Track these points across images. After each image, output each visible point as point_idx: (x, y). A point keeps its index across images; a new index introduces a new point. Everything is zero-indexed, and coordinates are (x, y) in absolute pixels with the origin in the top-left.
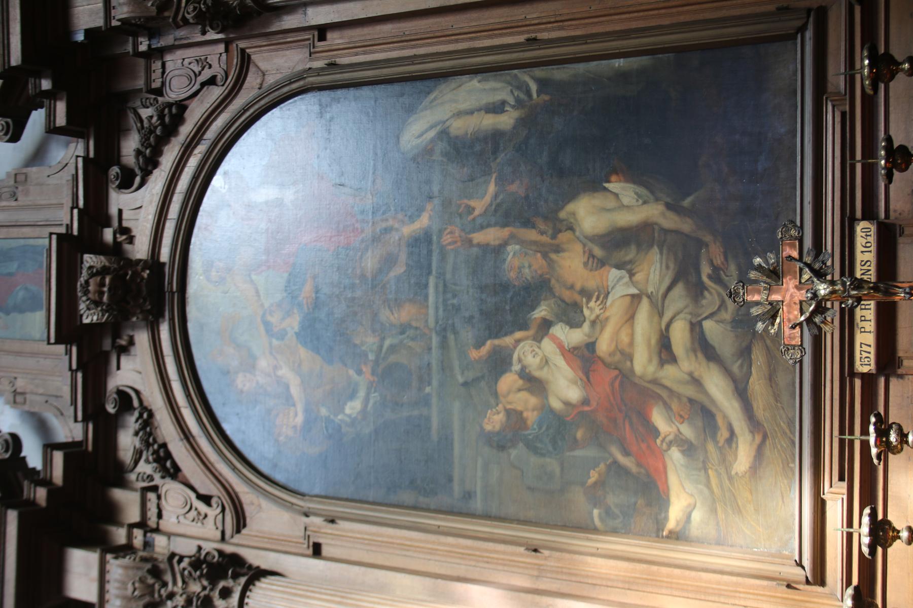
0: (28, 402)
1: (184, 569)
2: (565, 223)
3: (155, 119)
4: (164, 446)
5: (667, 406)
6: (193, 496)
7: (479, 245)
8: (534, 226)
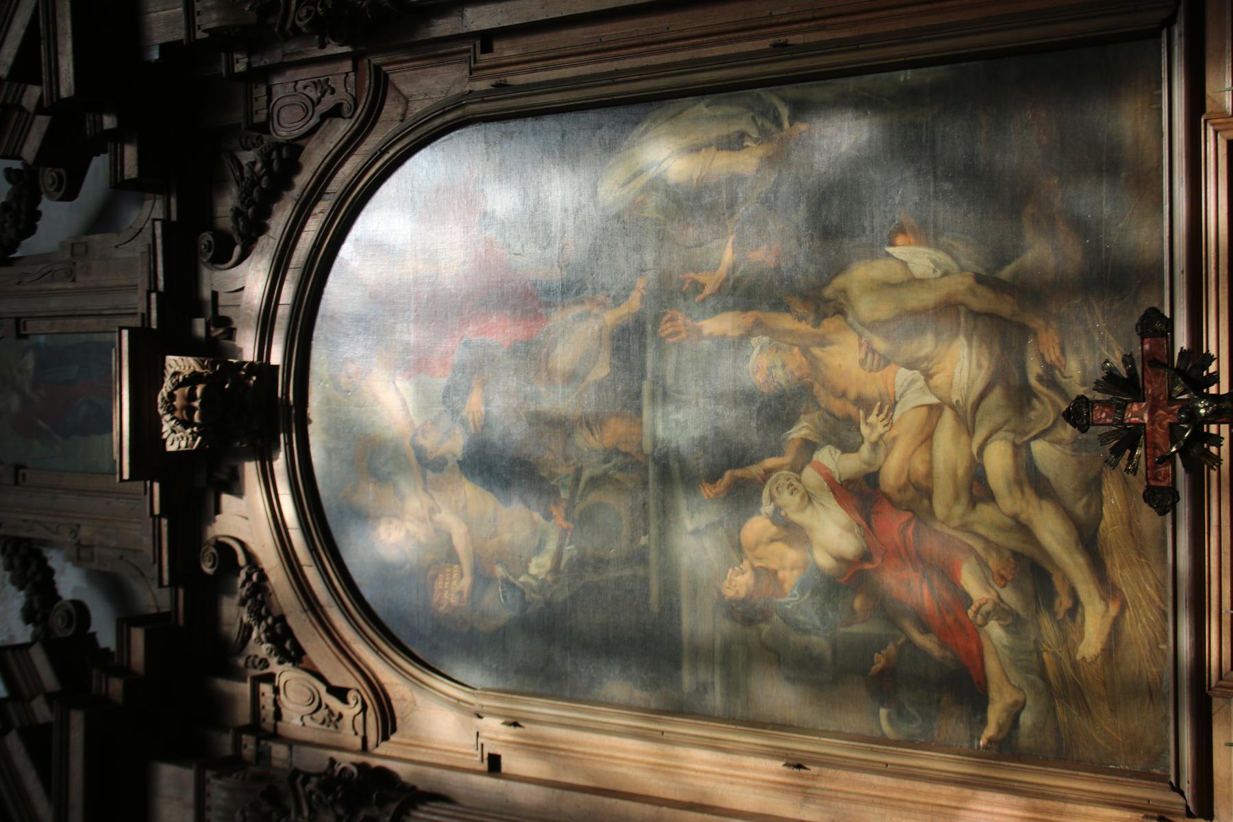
1: (311, 793)
2: (832, 304)
3: (259, 166)
4: (281, 619)
5: (982, 563)
6: (322, 688)
7: (711, 336)
8: (788, 310)
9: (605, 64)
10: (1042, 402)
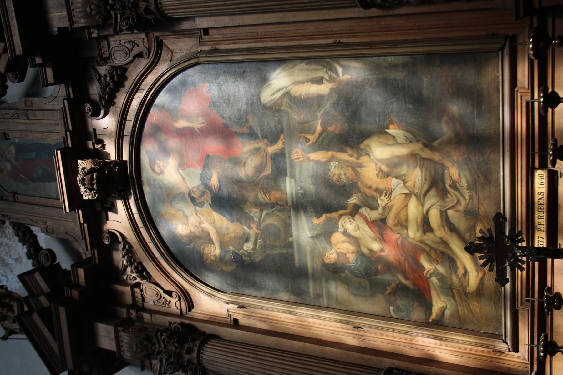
0: (55, 233)
1: (164, 339)
2: (364, 151)
3: (108, 78)
4: (141, 263)
5: (429, 255)
6: (161, 291)
7: (313, 160)
8: (345, 152)
9: (260, 44)
10: (451, 195)
